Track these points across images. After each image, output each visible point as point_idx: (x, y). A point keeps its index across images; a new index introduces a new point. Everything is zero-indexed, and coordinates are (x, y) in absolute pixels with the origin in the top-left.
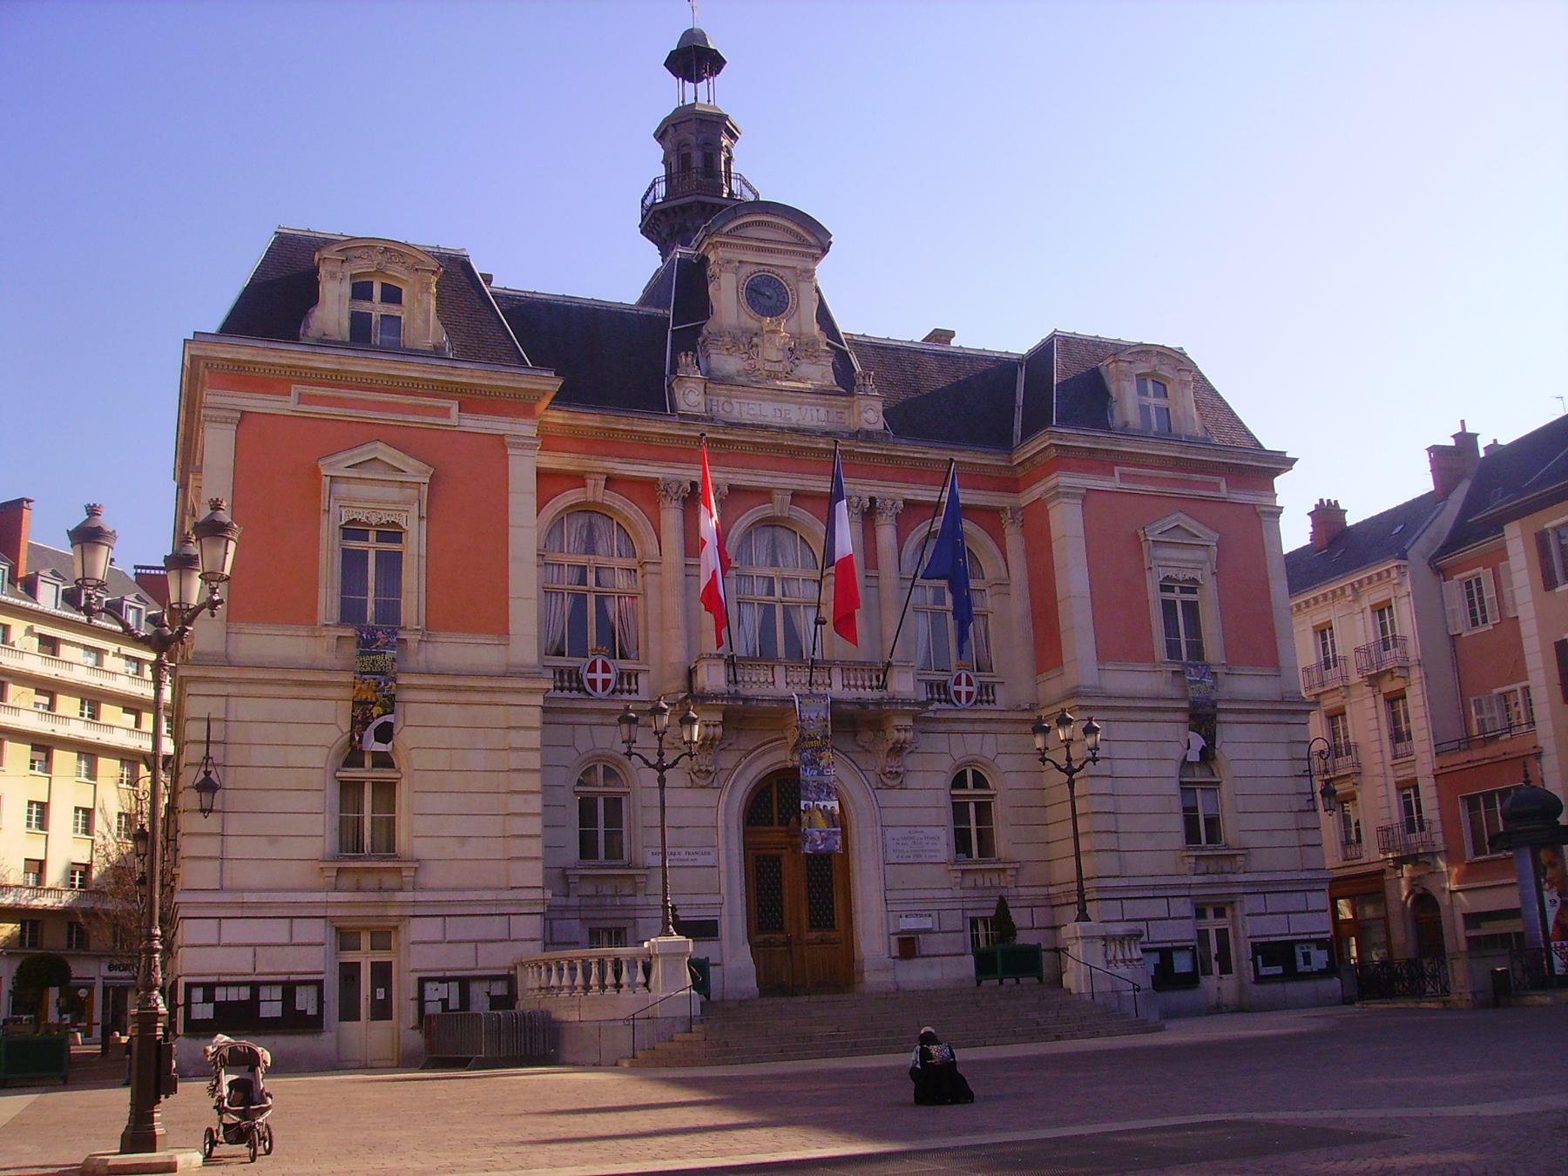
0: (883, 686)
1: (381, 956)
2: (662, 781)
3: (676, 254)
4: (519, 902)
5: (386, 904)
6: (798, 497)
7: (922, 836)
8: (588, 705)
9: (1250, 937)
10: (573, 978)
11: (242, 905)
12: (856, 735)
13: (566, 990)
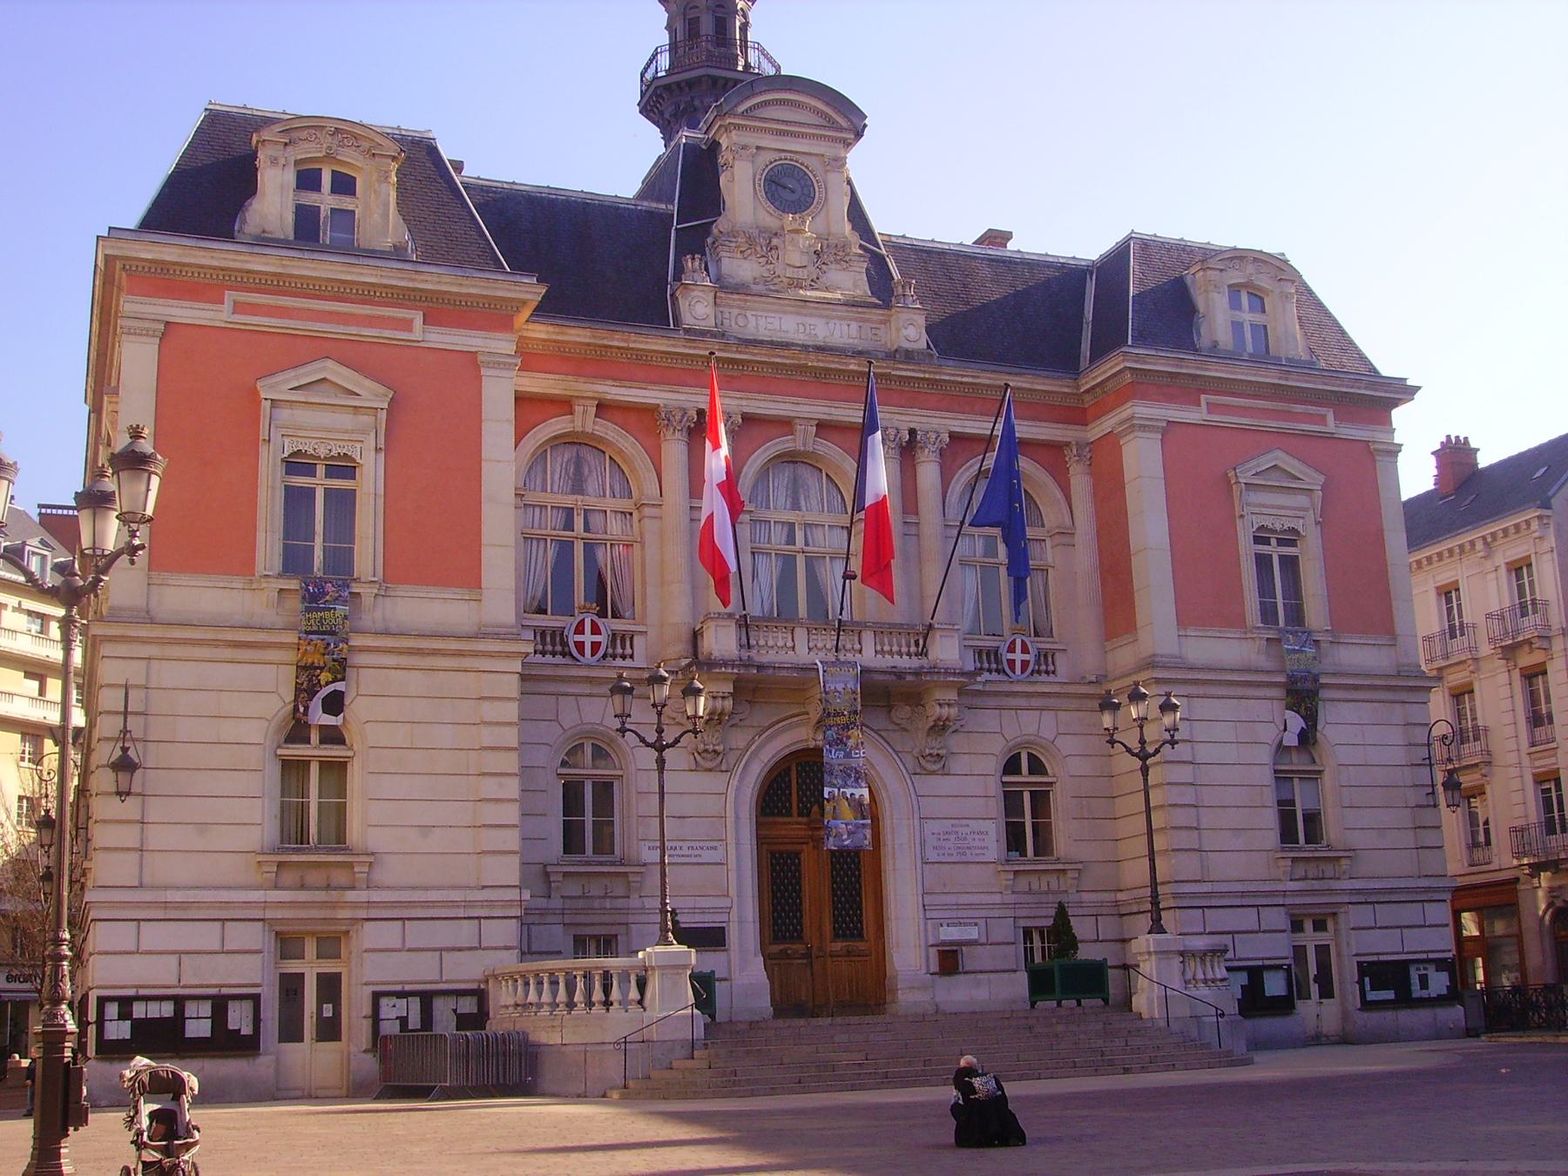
0: (923, 653)
1: (329, 967)
2: (661, 762)
3: (681, 138)
4: (490, 903)
5: (334, 905)
6: (824, 427)
8: (574, 672)
9: (1357, 955)
10: (554, 994)
11: (166, 905)
12: (890, 711)
13: (546, 1008)
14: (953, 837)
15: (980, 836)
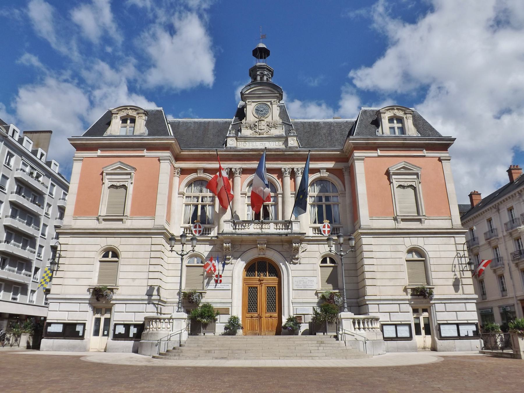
7: (307, 280)
12: (283, 246)
14: (302, 282)
15: (311, 282)
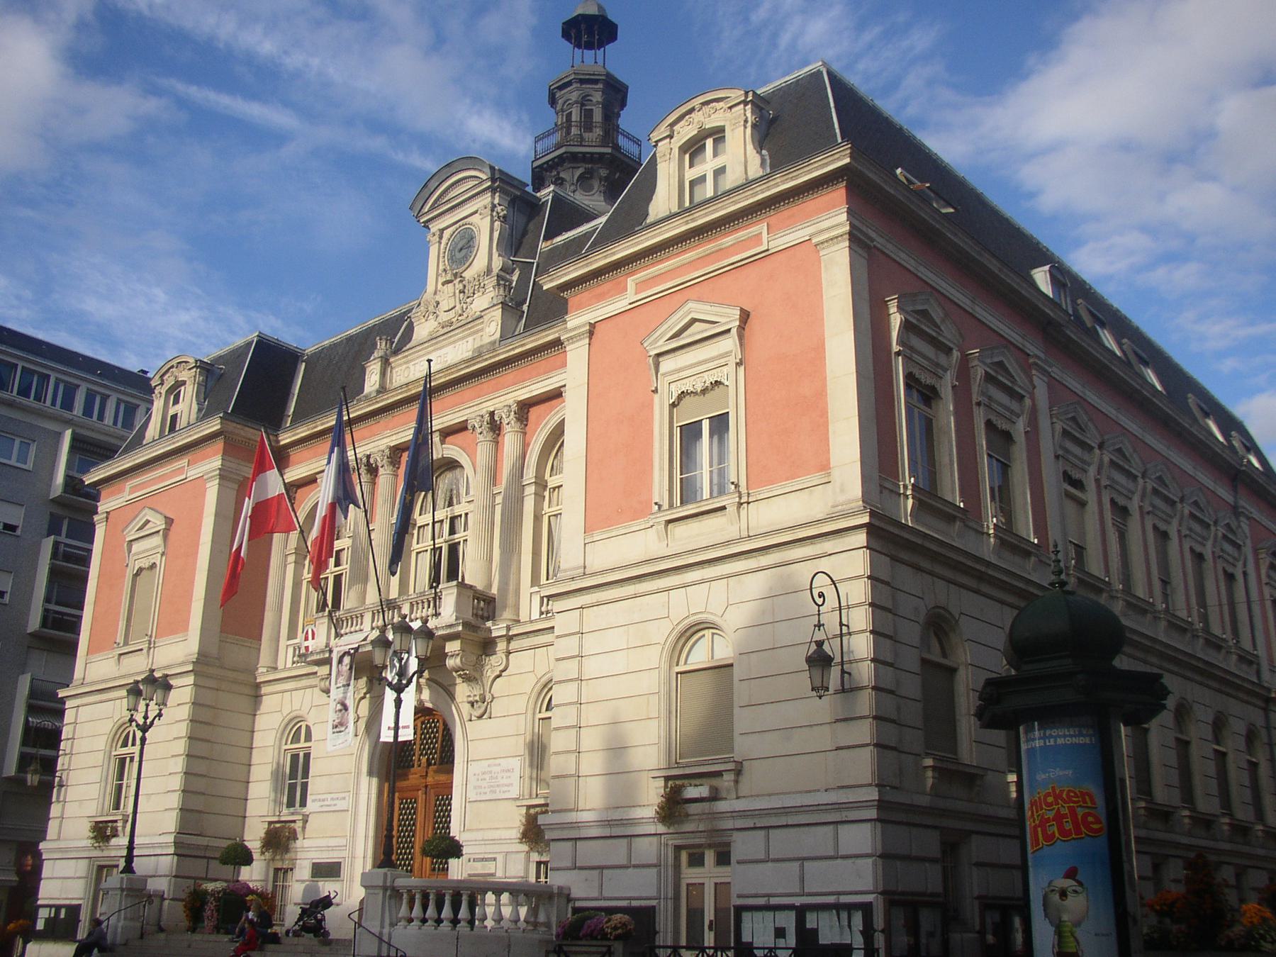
7: (497, 769)
10: (425, 908)
14: (487, 777)
15: (508, 774)
